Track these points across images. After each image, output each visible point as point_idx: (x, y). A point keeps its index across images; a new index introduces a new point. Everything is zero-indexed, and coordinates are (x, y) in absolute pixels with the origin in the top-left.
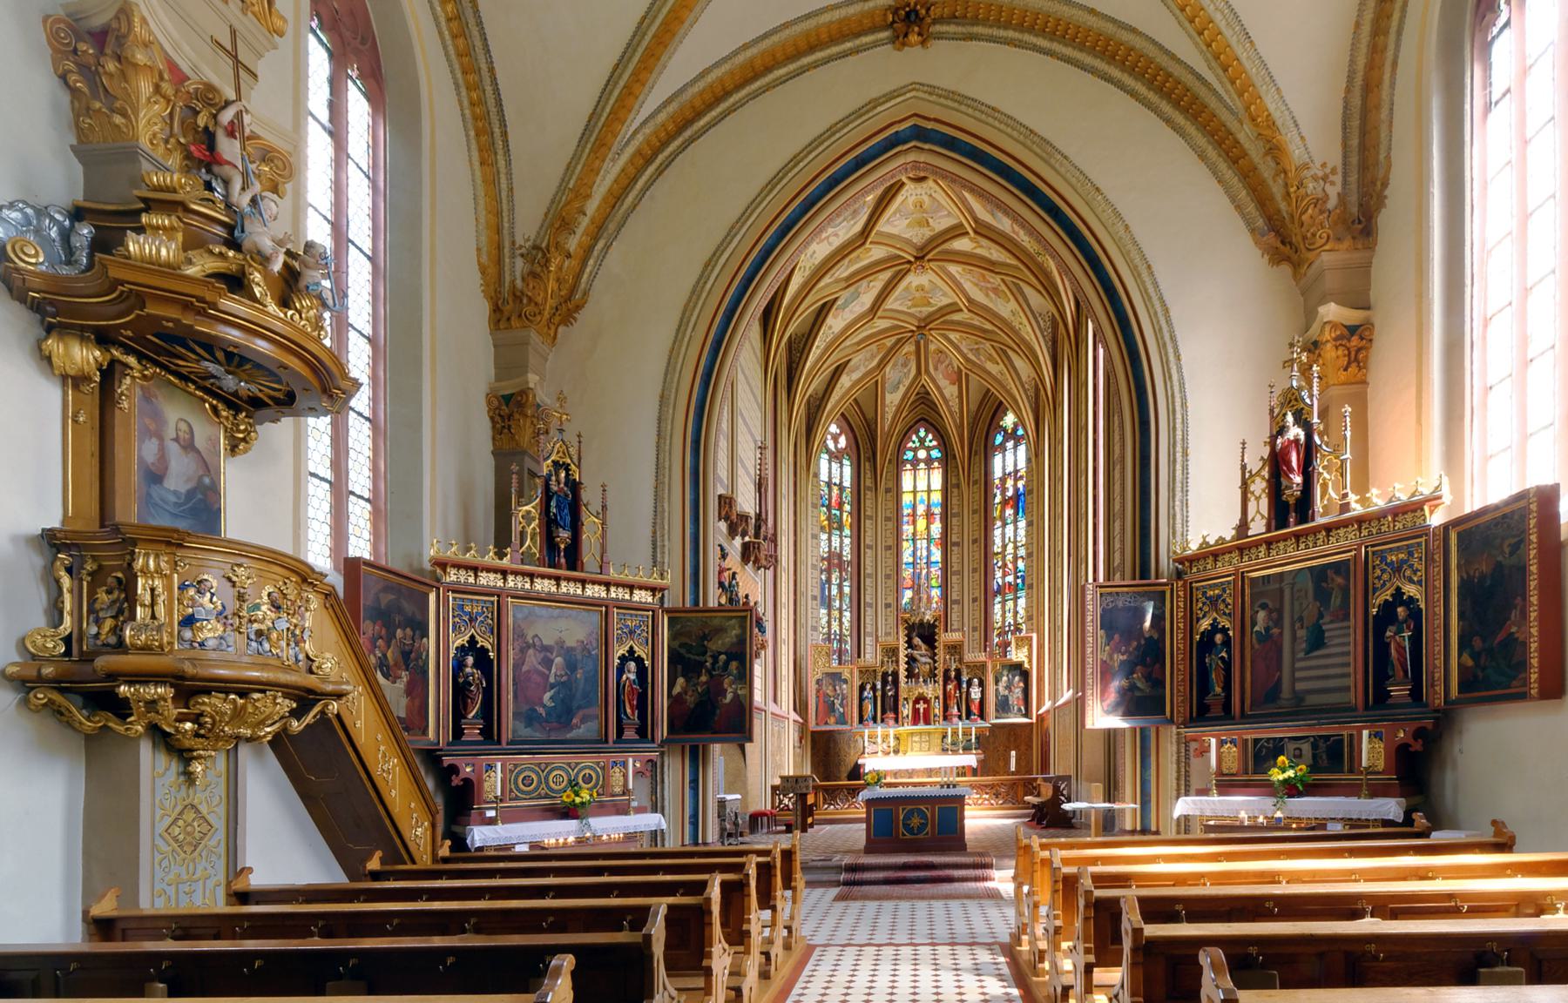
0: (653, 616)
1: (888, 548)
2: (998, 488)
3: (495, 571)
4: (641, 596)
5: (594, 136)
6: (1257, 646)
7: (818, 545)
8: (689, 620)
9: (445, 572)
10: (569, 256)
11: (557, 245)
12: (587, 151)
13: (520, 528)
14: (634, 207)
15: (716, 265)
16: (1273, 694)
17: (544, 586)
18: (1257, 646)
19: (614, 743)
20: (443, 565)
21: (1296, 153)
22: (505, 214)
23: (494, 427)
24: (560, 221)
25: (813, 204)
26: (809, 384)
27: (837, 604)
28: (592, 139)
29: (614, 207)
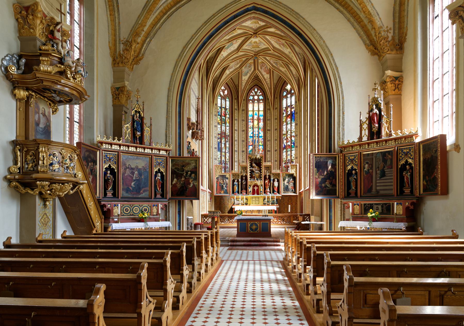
0: (166, 159)
1: (243, 131)
2: (284, 111)
3: (117, 145)
4: (163, 153)
5: (148, 8)
6: (365, 175)
7: (217, 129)
8: (178, 160)
9: (102, 145)
10: (138, 43)
11: (135, 41)
12: (145, 12)
13: (125, 131)
14: (159, 28)
15: (187, 48)
16: (370, 190)
17: (132, 149)
18: (365, 175)
19: (154, 199)
20: (102, 143)
21: (378, 23)
22: (117, 30)
23: (113, 98)
24: (135, 33)
25: (220, 29)
26: (214, 73)
27: (224, 150)
28: (147, 9)
29: (153, 28)
